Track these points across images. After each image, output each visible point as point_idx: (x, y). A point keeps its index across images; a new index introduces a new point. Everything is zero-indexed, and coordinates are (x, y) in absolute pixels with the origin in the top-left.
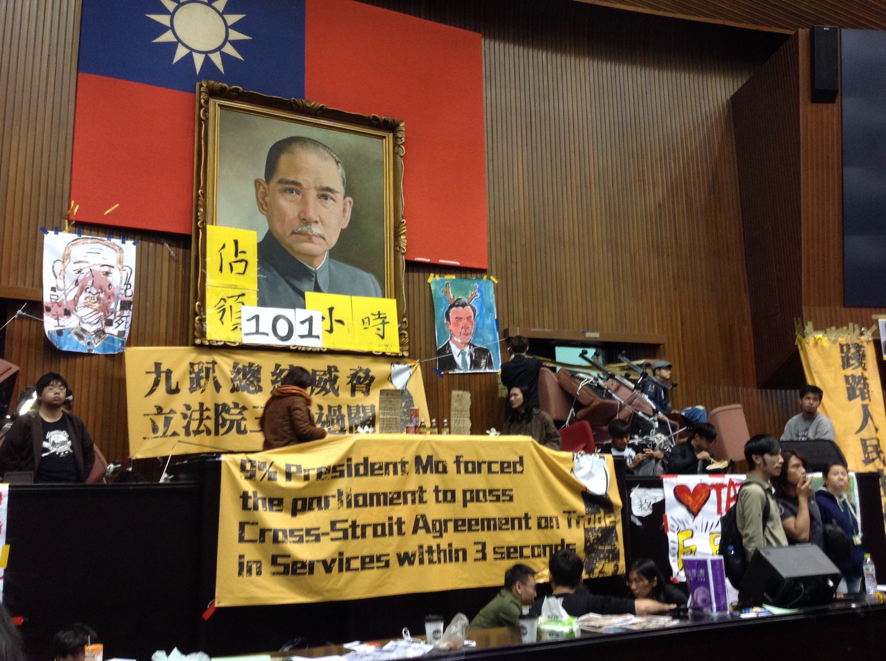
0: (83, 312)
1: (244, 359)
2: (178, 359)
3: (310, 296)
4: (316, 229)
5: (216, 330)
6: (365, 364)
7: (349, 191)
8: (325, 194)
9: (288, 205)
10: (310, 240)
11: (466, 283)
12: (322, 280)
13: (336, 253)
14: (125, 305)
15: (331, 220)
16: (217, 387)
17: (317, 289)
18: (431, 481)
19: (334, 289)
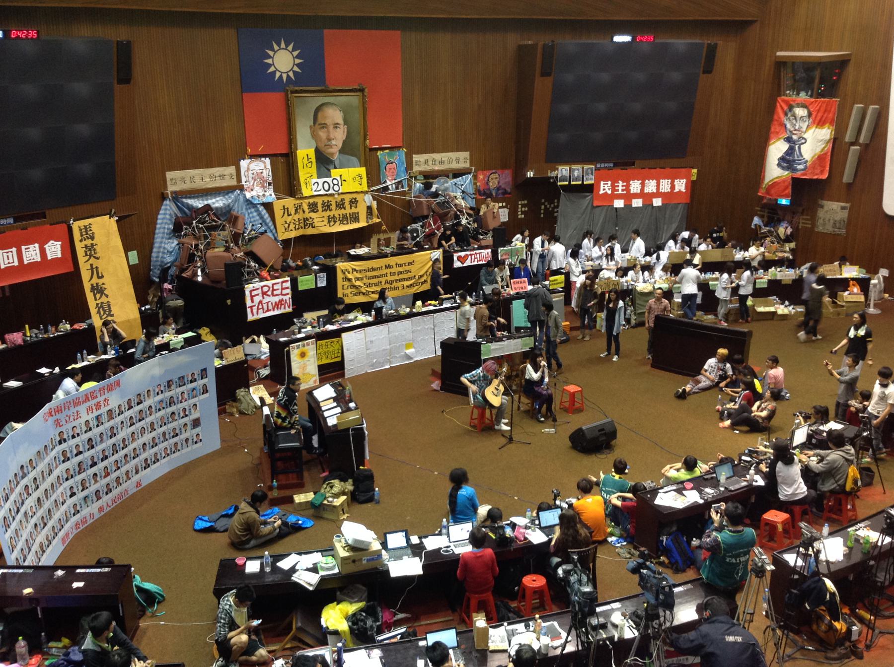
1: (311, 201)
2: (290, 202)
3: (333, 171)
4: (334, 142)
6: (354, 196)
7: (346, 122)
8: (336, 126)
9: (322, 134)
11: (393, 153)
12: (337, 163)
13: (342, 151)
14: (270, 184)
15: (339, 137)
16: (304, 212)
17: (335, 168)
18: (388, 271)
19: (342, 167)
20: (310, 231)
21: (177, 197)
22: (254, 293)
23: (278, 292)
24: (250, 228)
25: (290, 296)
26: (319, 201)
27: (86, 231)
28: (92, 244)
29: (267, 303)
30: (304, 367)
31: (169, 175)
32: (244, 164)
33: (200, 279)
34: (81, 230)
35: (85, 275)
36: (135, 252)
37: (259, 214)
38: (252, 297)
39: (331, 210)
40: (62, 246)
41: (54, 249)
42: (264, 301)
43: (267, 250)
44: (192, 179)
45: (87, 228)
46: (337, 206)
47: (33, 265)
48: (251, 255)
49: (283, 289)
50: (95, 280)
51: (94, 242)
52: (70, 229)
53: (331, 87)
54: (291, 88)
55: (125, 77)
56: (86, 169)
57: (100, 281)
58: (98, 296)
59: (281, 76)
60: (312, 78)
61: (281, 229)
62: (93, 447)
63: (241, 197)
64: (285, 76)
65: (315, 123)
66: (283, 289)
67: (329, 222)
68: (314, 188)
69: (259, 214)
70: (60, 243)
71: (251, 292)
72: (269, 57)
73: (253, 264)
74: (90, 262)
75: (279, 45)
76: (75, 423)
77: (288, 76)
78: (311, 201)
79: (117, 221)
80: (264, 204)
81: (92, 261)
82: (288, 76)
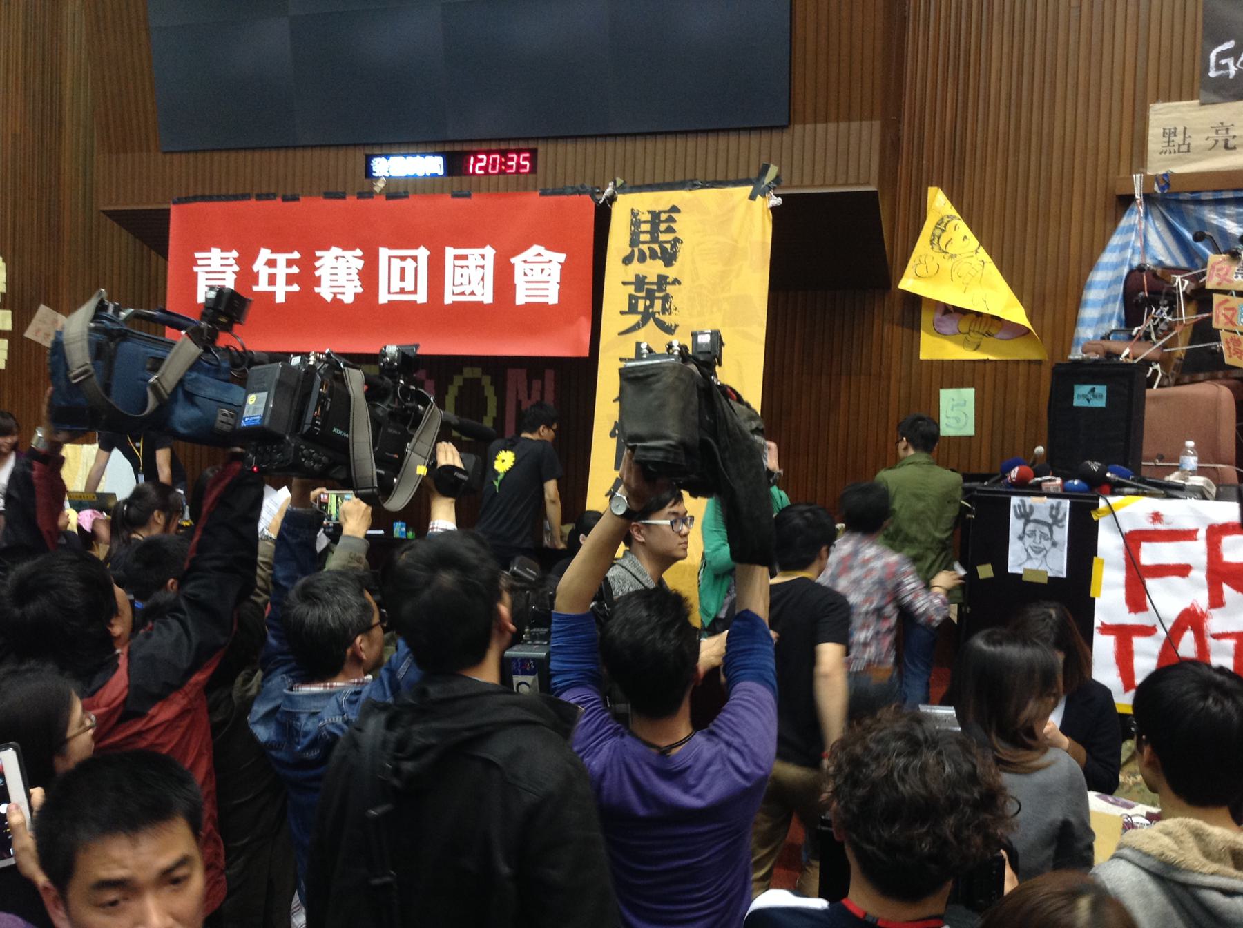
22: (1150, 554)
27: (654, 232)
28: (662, 280)
34: (636, 223)
36: (969, 393)
40: (564, 266)
41: (540, 275)
42: (1216, 622)
47: (468, 313)
51: (671, 273)
52: (603, 217)
70: (562, 257)
71: (1133, 540)
79: (774, 209)
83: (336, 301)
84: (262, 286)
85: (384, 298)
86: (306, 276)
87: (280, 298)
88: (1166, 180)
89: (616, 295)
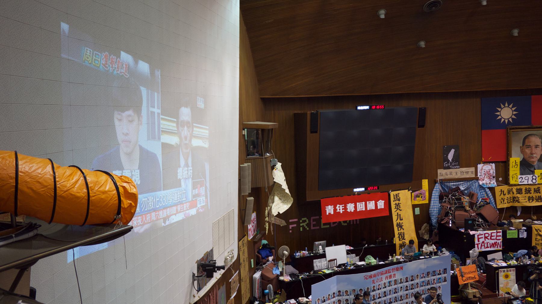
0: (486, 179)
1: (518, 187)
2: (505, 188)
4: (534, 155)
5: (512, 182)
8: (537, 146)
9: (528, 151)
10: (533, 158)
13: (539, 161)
14: (494, 177)
16: (513, 193)
19: (538, 169)
20: (516, 204)
21: (442, 182)
22: (480, 237)
23: (495, 238)
24: (480, 200)
25: (501, 241)
26: (524, 188)
29: (487, 243)
30: (507, 283)
31: (439, 171)
32: (480, 166)
33: (450, 225)
35: (395, 218)
36: (418, 208)
37: (486, 193)
38: (478, 239)
39: (530, 193)
41: (381, 204)
42: (485, 242)
43: (488, 213)
44: (451, 174)
45: (397, 195)
46: (535, 191)
47: (371, 211)
48: (480, 215)
49: (497, 236)
50: (399, 221)
52: (389, 195)
53: (535, 126)
54: (510, 127)
55: (422, 125)
56: (399, 167)
57: (401, 222)
58: (399, 229)
59: (504, 121)
60: (523, 121)
61: (498, 202)
62: (386, 296)
63: (477, 184)
64: (506, 121)
65: (523, 144)
66: (497, 236)
67: (529, 200)
68: (520, 180)
69: (486, 193)
71: (478, 236)
72: (498, 111)
73: (480, 220)
74: (397, 212)
75: (504, 105)
76: (380, 283)
77: (509, 121)
78: (518, 187)
80: (489, 188)
81: (398, 211)
82: (509, 121)
83: (351, 212)
84: (338, 211)
85: (358, 210)
86: (345, 208)
87: (341, 212)
88: (441, 180)
89: (393, 206)
